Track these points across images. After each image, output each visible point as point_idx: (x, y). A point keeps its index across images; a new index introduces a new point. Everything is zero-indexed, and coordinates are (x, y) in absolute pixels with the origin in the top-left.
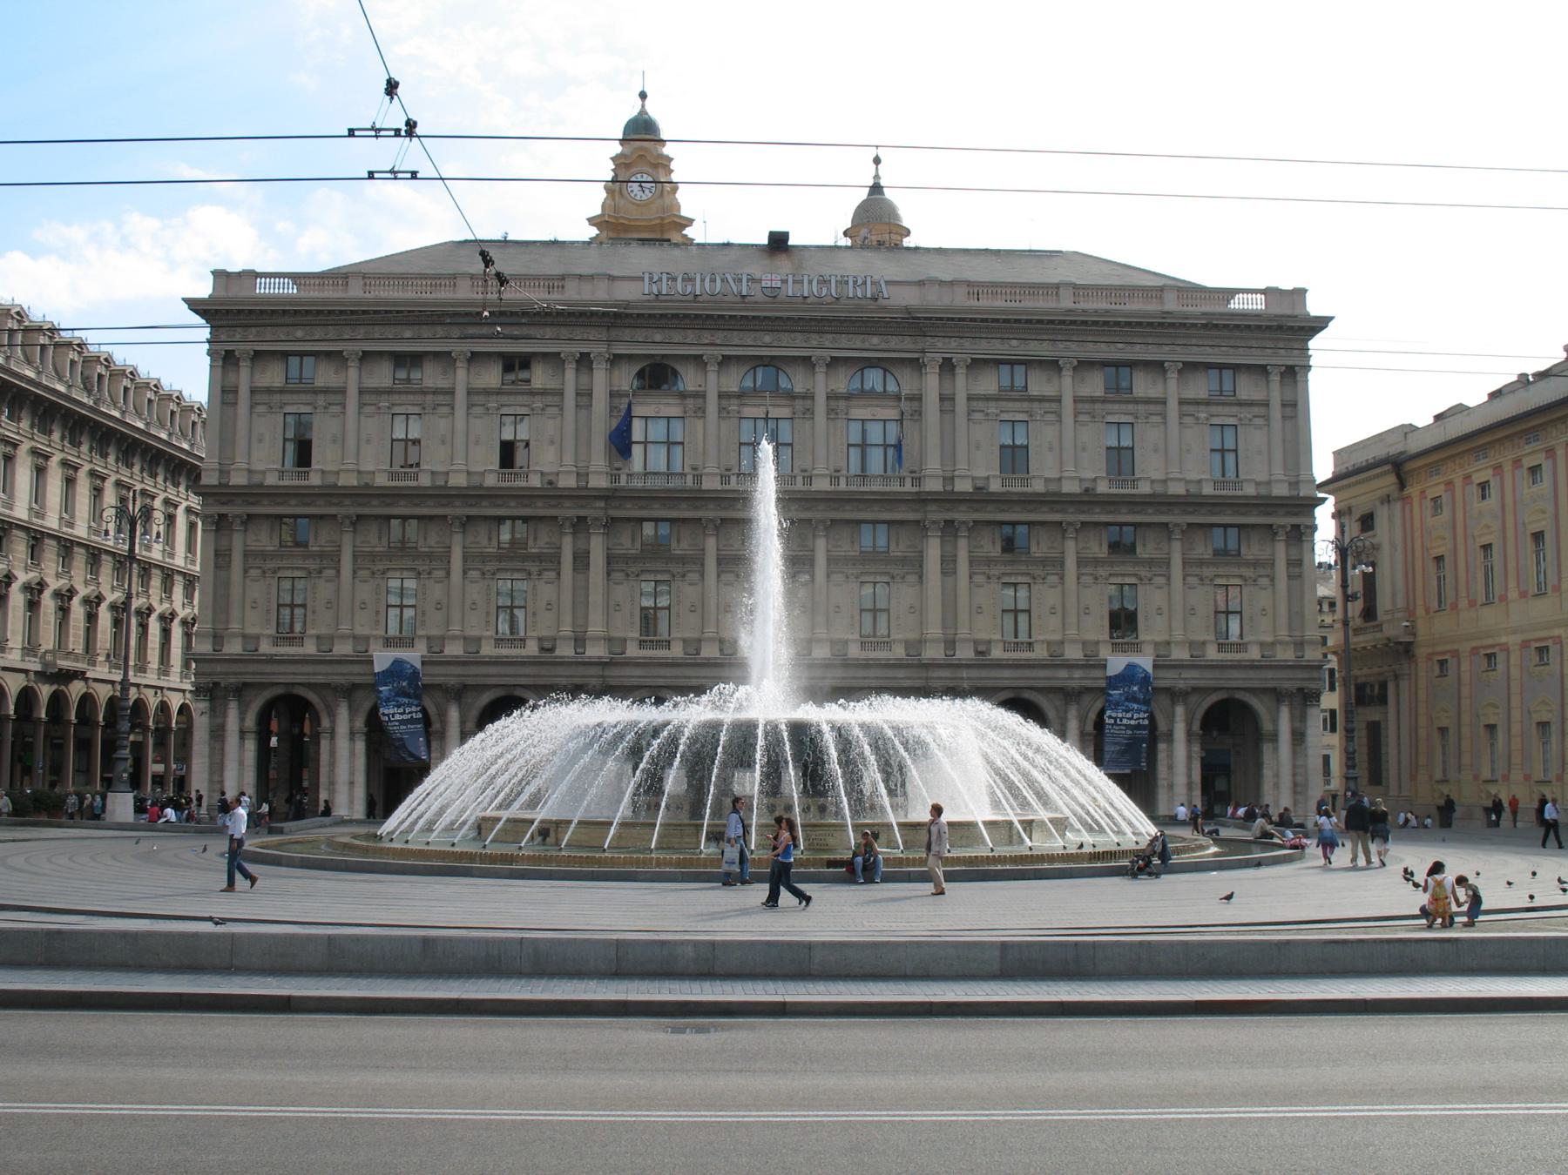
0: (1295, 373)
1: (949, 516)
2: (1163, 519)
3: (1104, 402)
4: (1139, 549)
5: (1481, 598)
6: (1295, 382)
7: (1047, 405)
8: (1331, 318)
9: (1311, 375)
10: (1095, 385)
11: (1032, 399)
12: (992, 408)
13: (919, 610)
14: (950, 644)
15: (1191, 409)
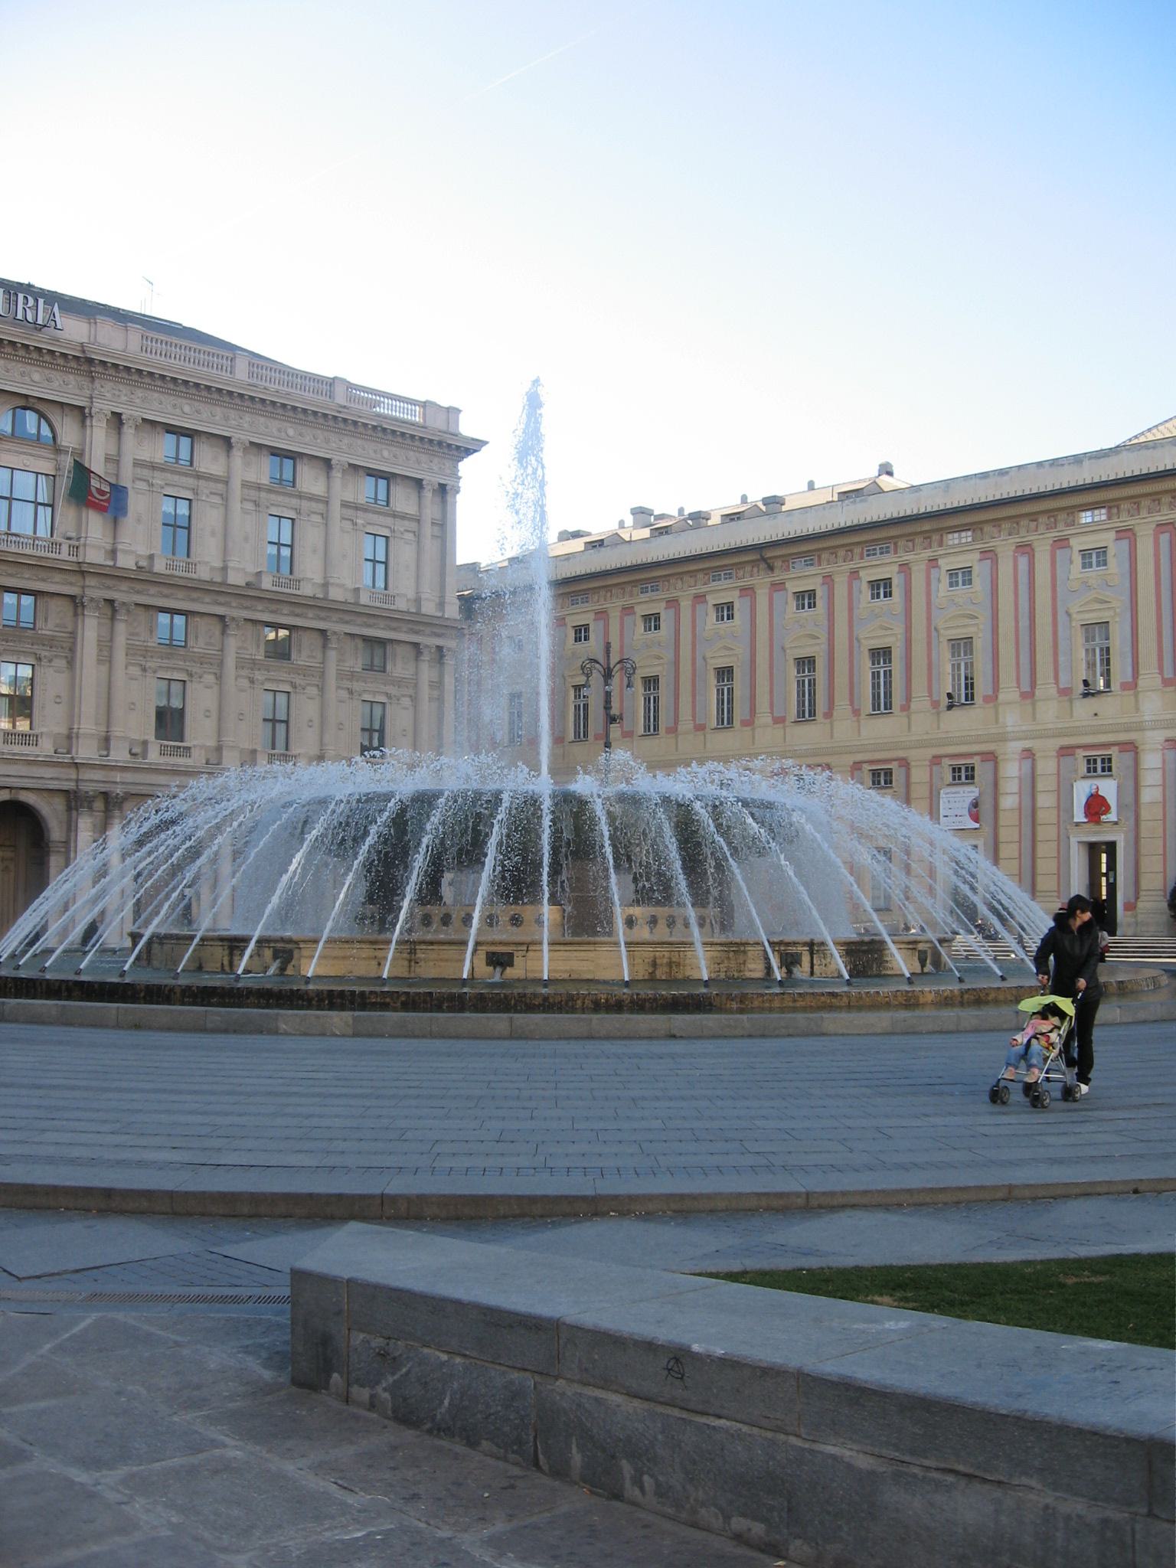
0: (445, 492)
1: (110, 595)
2: (322, 625)
3: (270, 491)
4: (294, 656)
5: (571, 736)
6: (444, 501)
7: (212, 484)
8: (485, 443)
9: (458, 496)
10: (263, 470)
11: (199, 476)
12: (158, 479)
13: (72, 702)
14: (106, 741)
15: (350, 513)
